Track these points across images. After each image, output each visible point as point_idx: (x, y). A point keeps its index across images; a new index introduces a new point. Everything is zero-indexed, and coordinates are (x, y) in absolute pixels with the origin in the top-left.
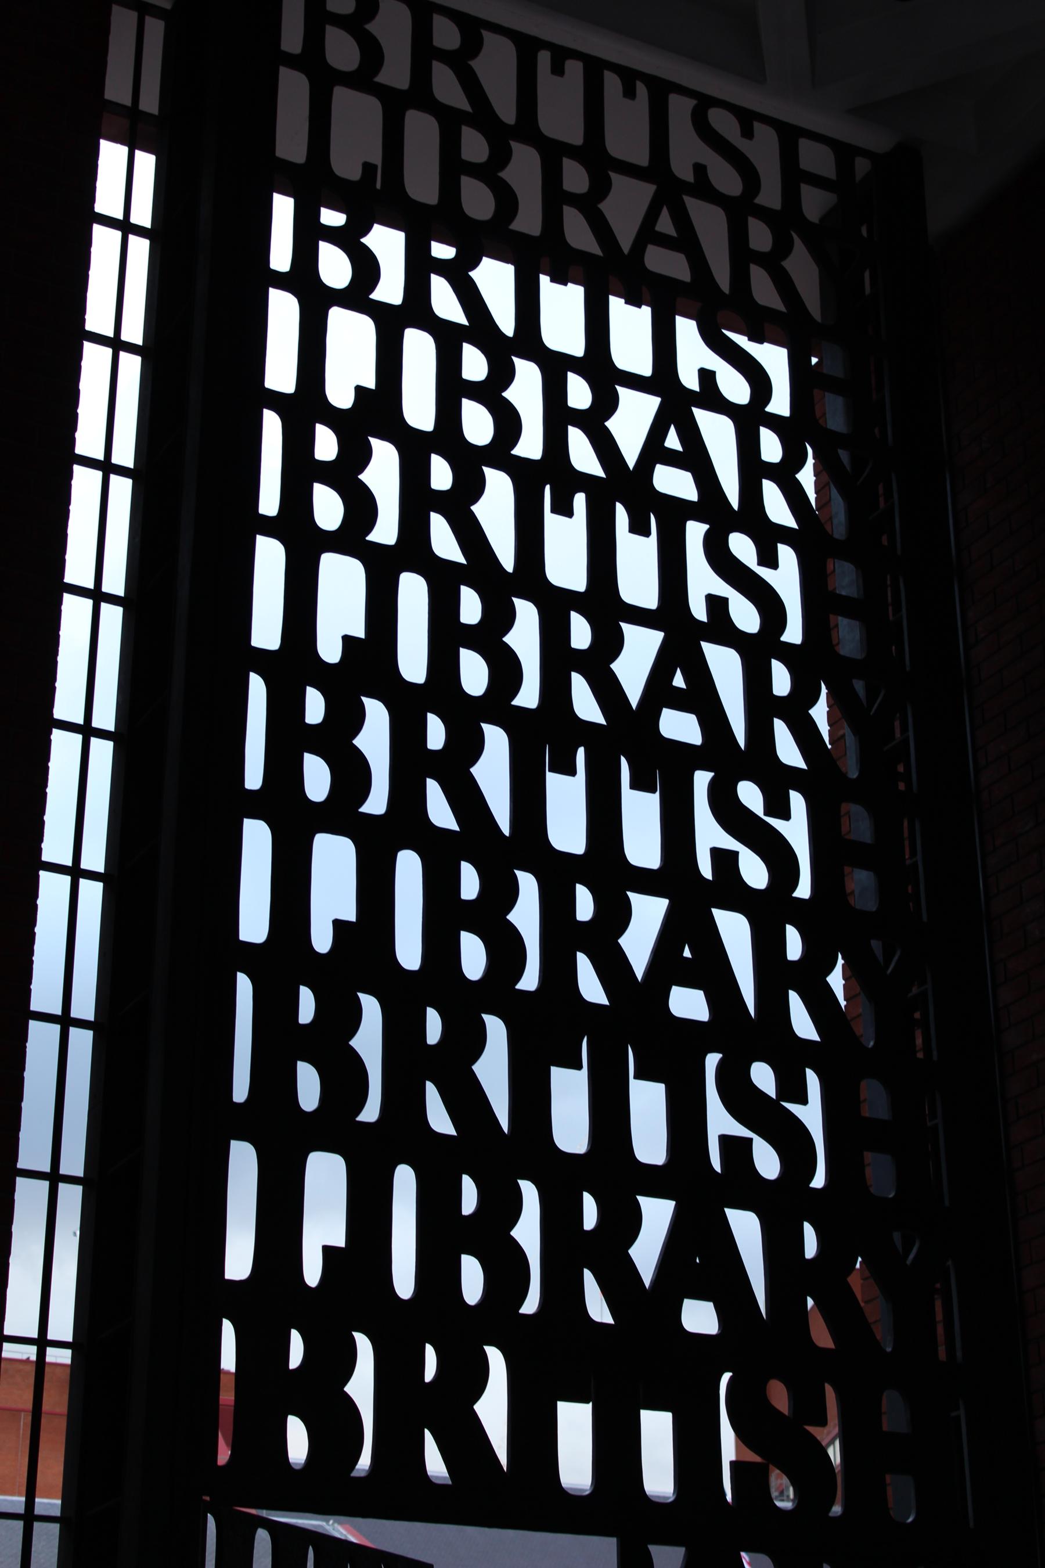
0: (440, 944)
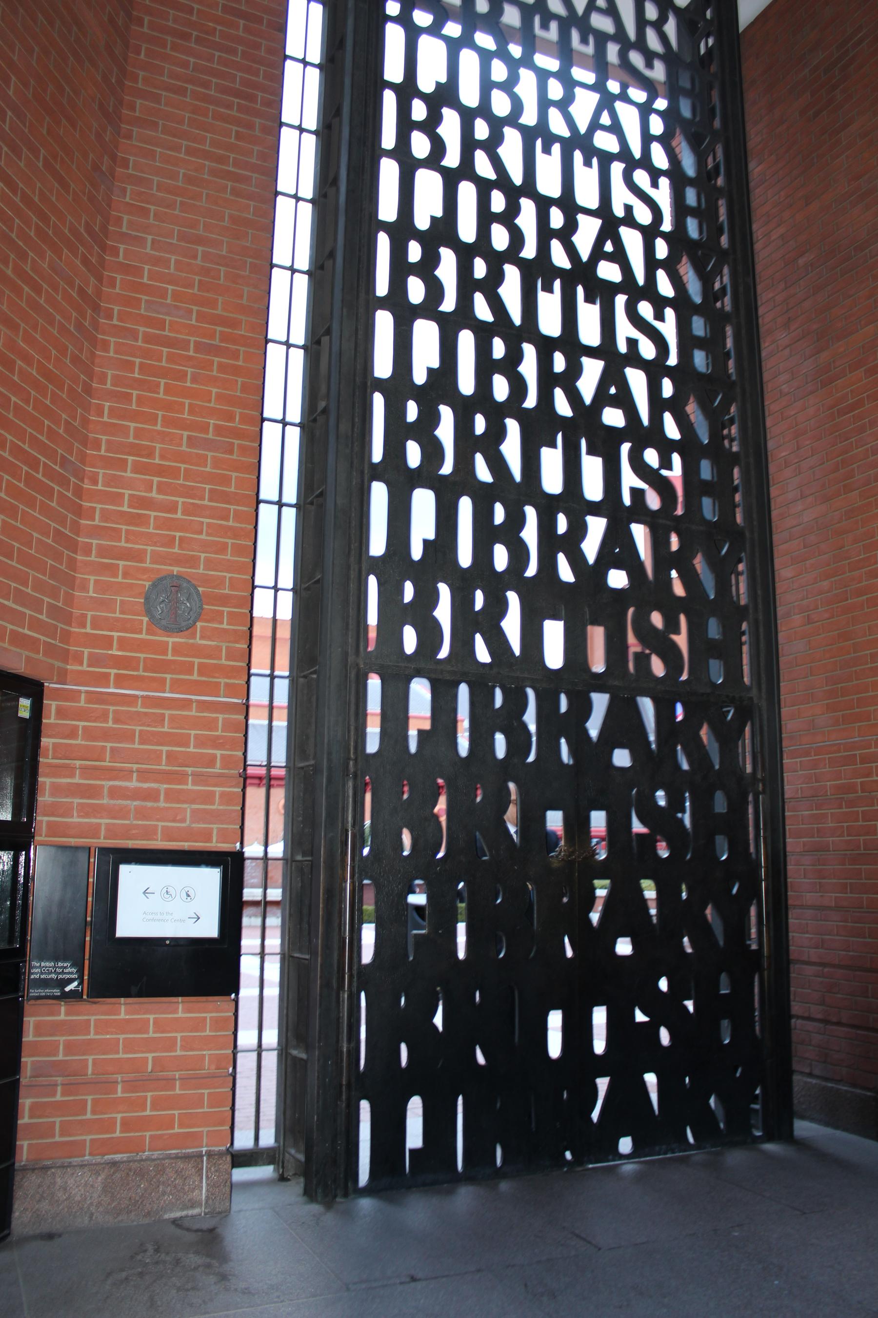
0: (483, 552)
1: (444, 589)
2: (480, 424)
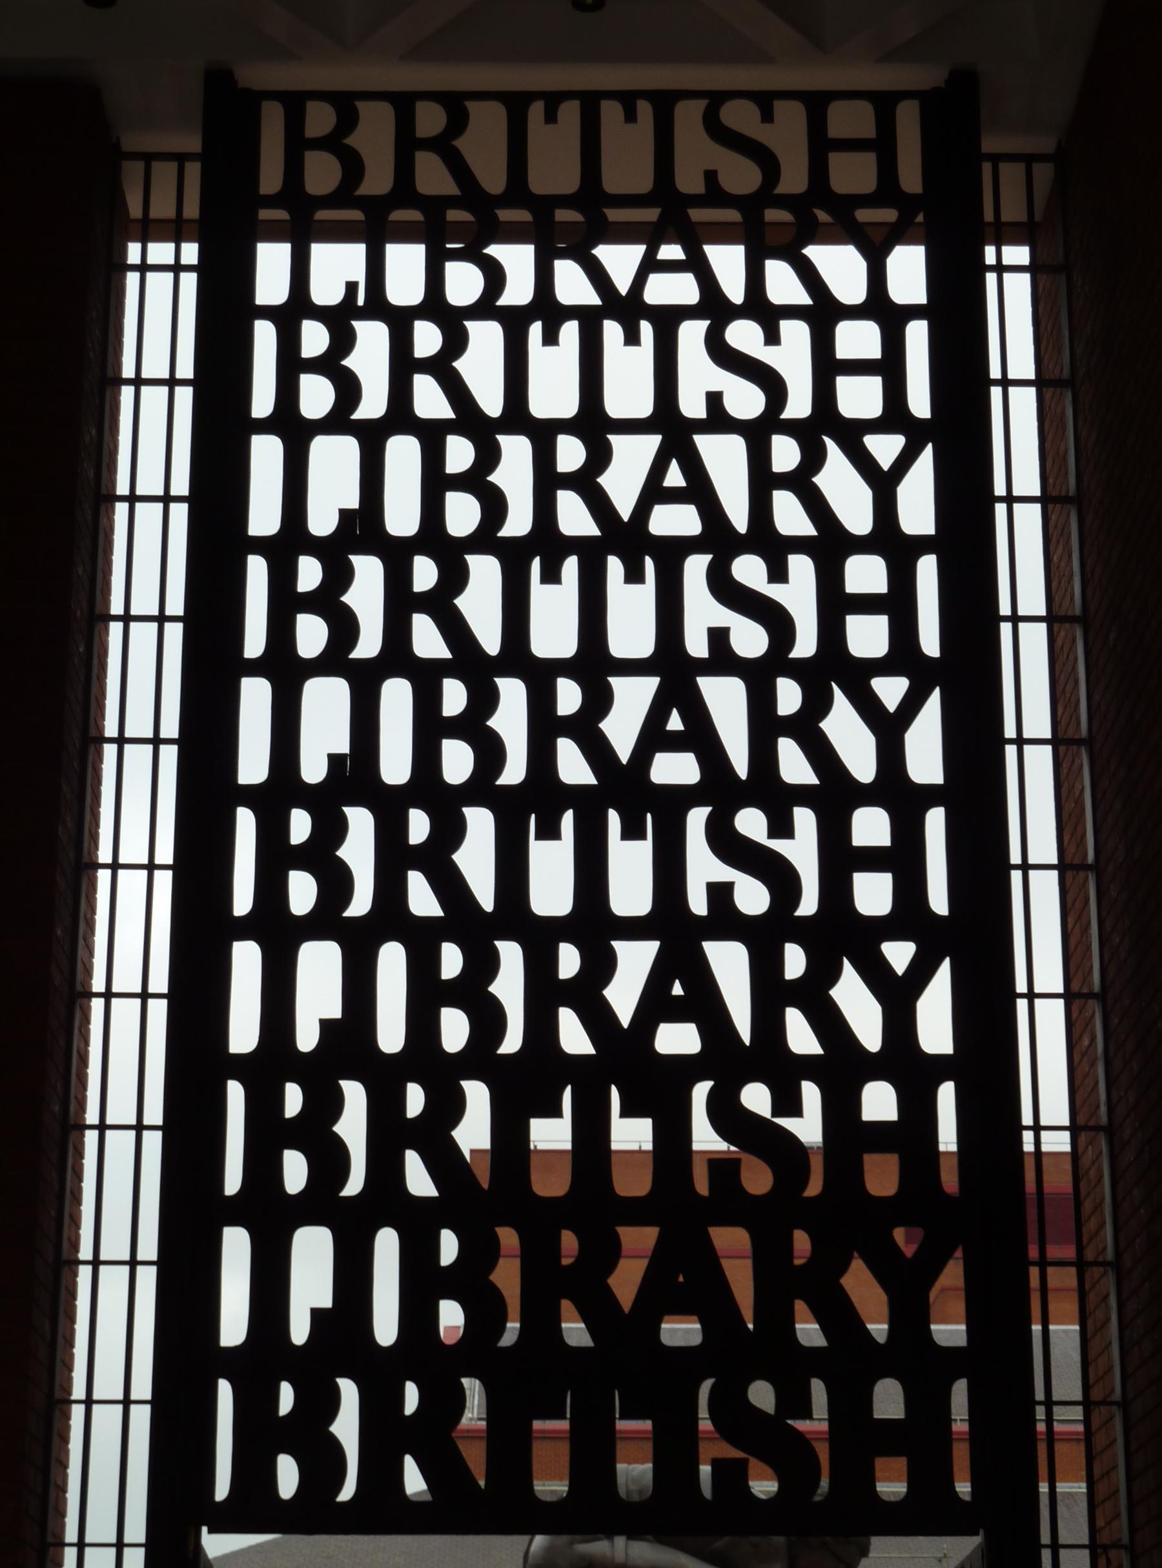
1: (348, 1390)
2: (415, 1099)
